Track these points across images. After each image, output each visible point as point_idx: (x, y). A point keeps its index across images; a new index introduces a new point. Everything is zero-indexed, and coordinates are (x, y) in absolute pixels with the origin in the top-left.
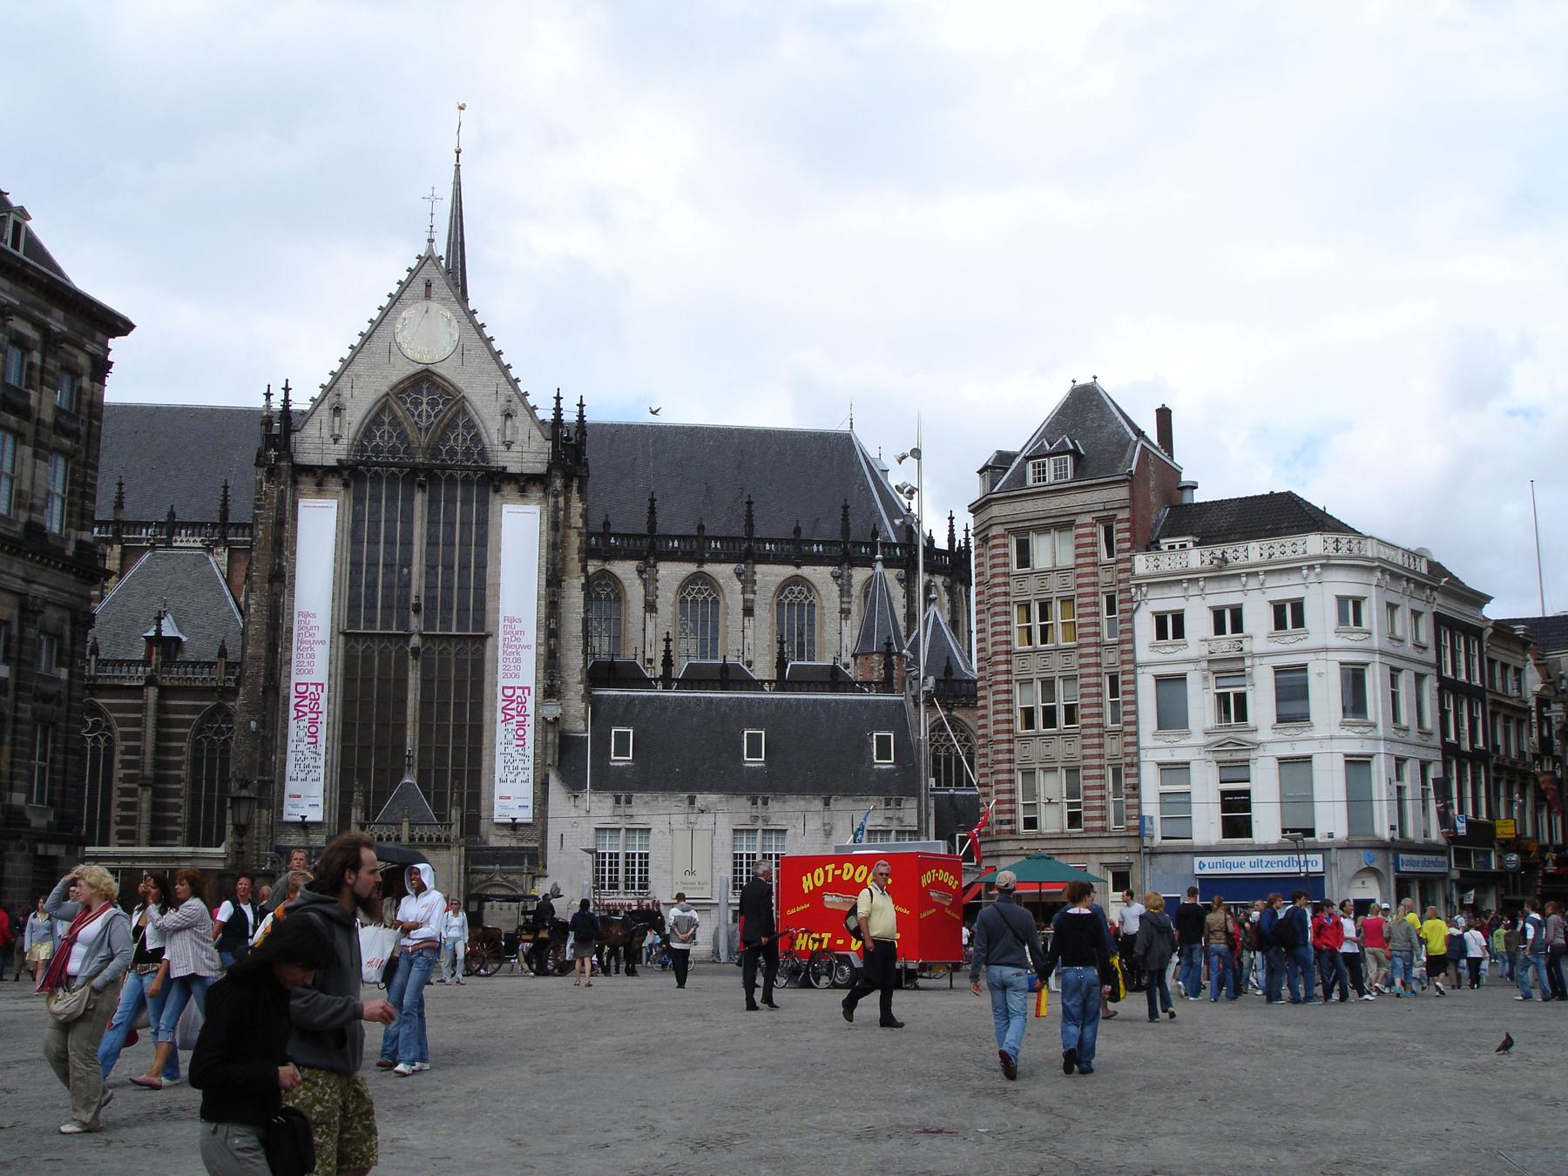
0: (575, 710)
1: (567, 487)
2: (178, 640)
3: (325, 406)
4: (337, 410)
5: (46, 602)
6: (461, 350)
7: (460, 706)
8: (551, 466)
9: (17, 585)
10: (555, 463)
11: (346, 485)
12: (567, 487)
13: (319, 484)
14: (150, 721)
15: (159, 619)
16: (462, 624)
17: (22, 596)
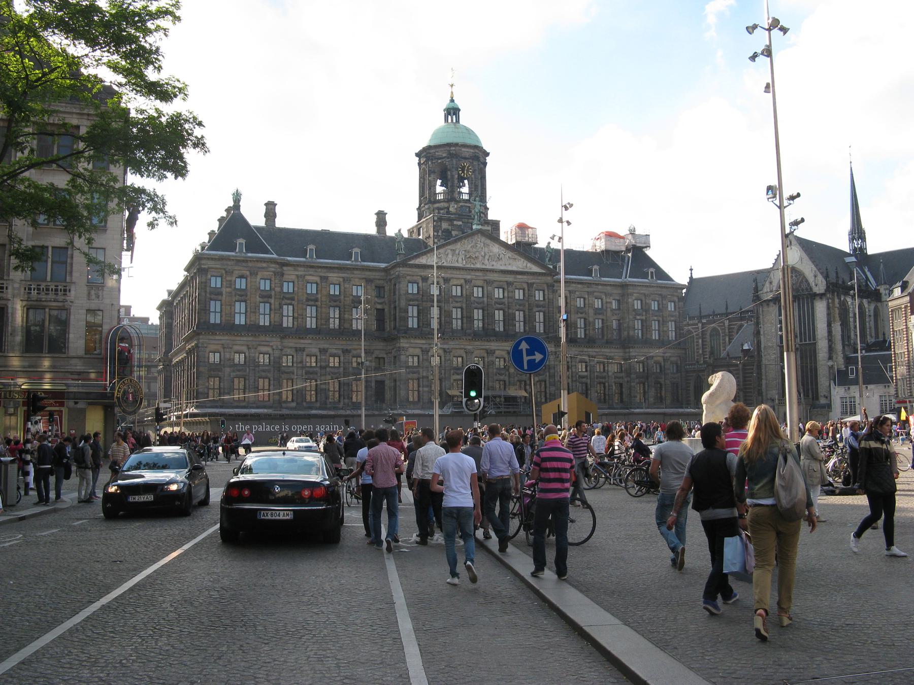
0: (839, 361)
1: (833, 295)
2: (750, 349)
3: (767, 282)
4: (771, 283)
5: (670, 357)
6: (801, 259)
7: (811, 363)
8: (826, 291)
9: (662, 354)
10: (828, 289)
11: (775, 304)
12: (833, 295)
13: (768, 305)
14: (741, 373)
15: (742, 345)
16: (810, 340)
17: (663, 357)
